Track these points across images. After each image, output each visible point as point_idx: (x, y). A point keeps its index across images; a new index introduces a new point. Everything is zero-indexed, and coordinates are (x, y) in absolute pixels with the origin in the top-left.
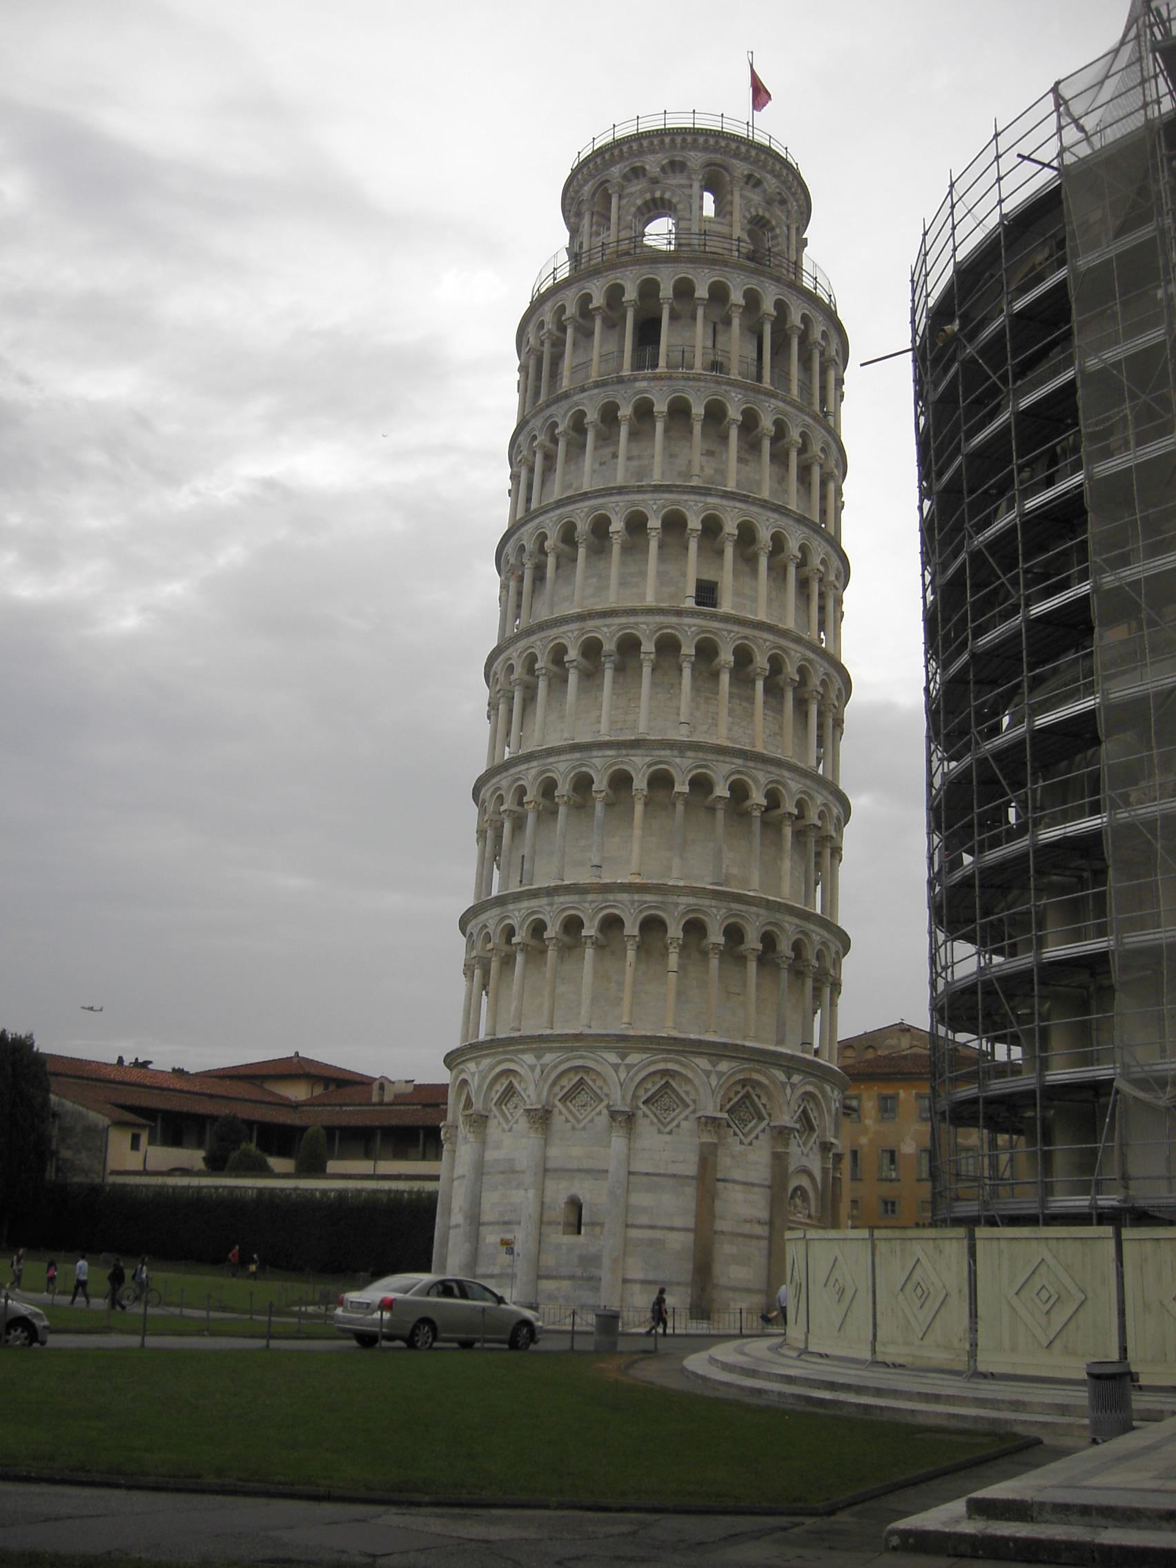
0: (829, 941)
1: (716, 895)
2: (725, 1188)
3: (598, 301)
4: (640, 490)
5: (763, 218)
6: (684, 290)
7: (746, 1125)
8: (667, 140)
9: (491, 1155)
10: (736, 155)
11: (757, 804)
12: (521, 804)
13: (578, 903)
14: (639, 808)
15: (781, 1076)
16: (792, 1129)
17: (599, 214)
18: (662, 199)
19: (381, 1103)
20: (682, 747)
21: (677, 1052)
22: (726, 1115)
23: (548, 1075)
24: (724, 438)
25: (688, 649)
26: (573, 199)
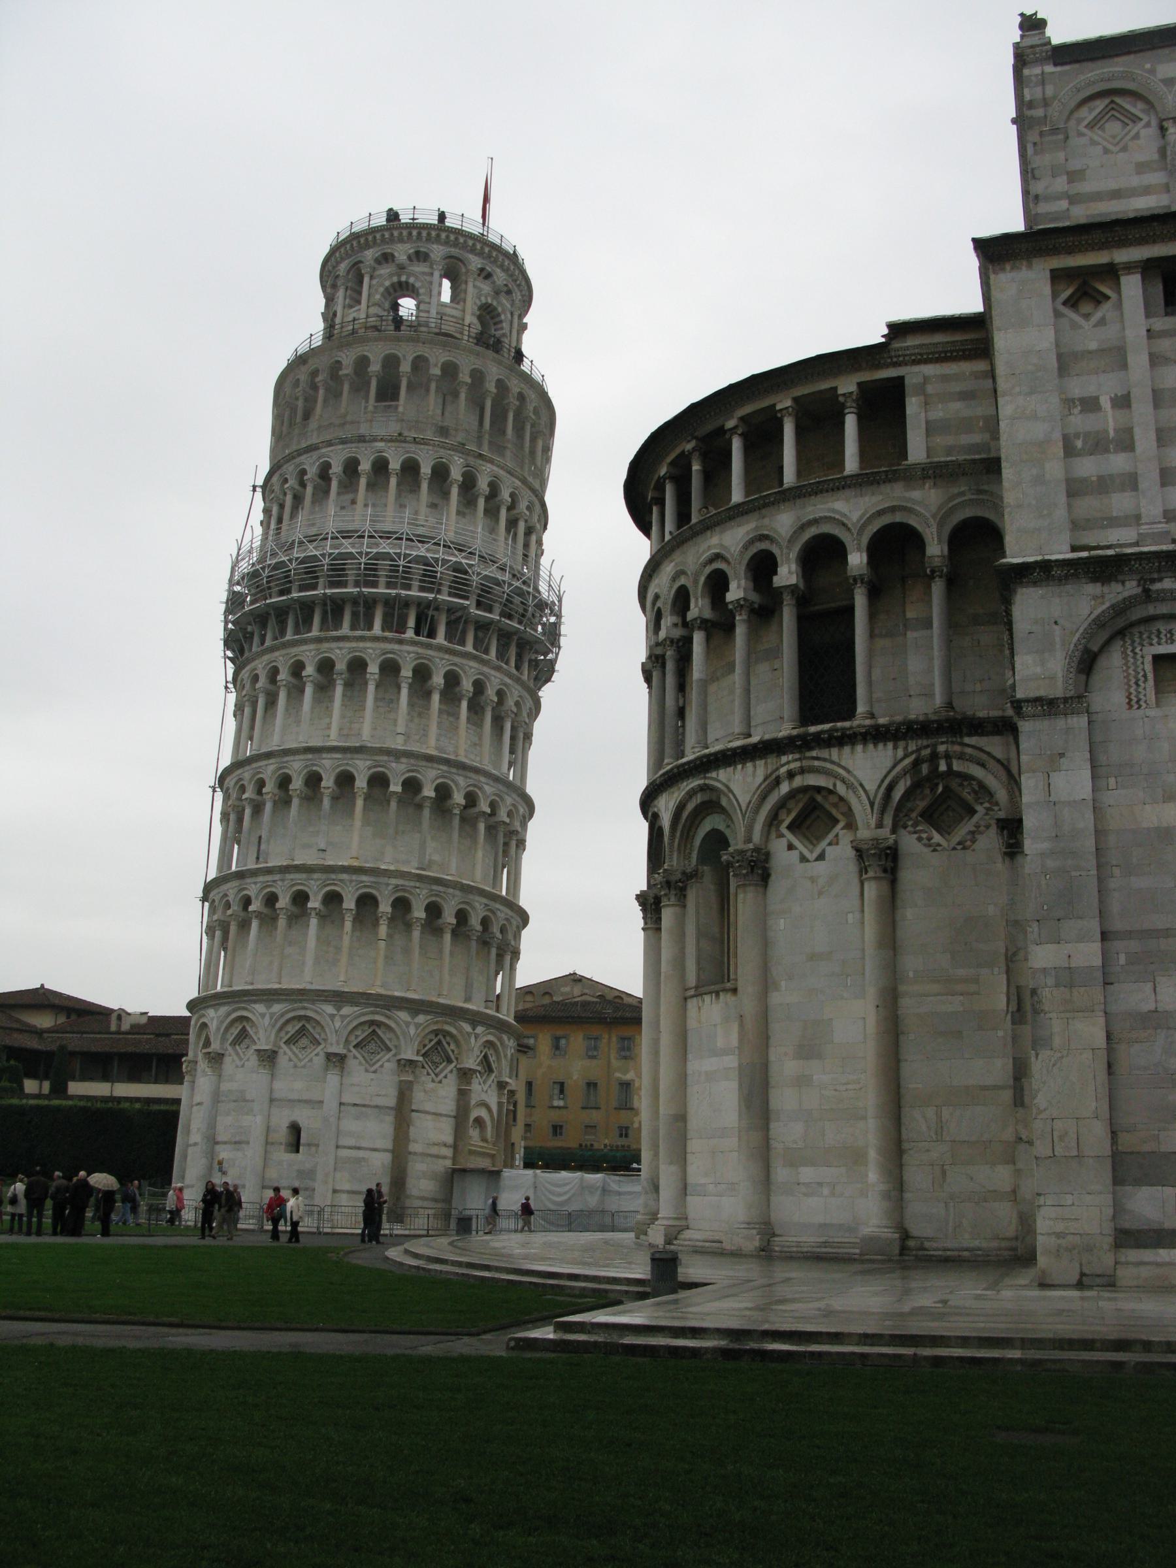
1: (420, 878)
3: (347, 370)
6: (419, 363)
8: (415, 233)
9: (225, 1086)
10: (473, 250)
12: (260, 793)
14: (360, 803)
15: (467, 1027)
16: (475, 1071)
17: (352, 289)
18: (407, 283)
19: (118, 1032)
20: (397, 754)
22: (421, 1059)
23: (276, 1021)
24: (446, 495)
25: (407, 673)
26: (330, 272)
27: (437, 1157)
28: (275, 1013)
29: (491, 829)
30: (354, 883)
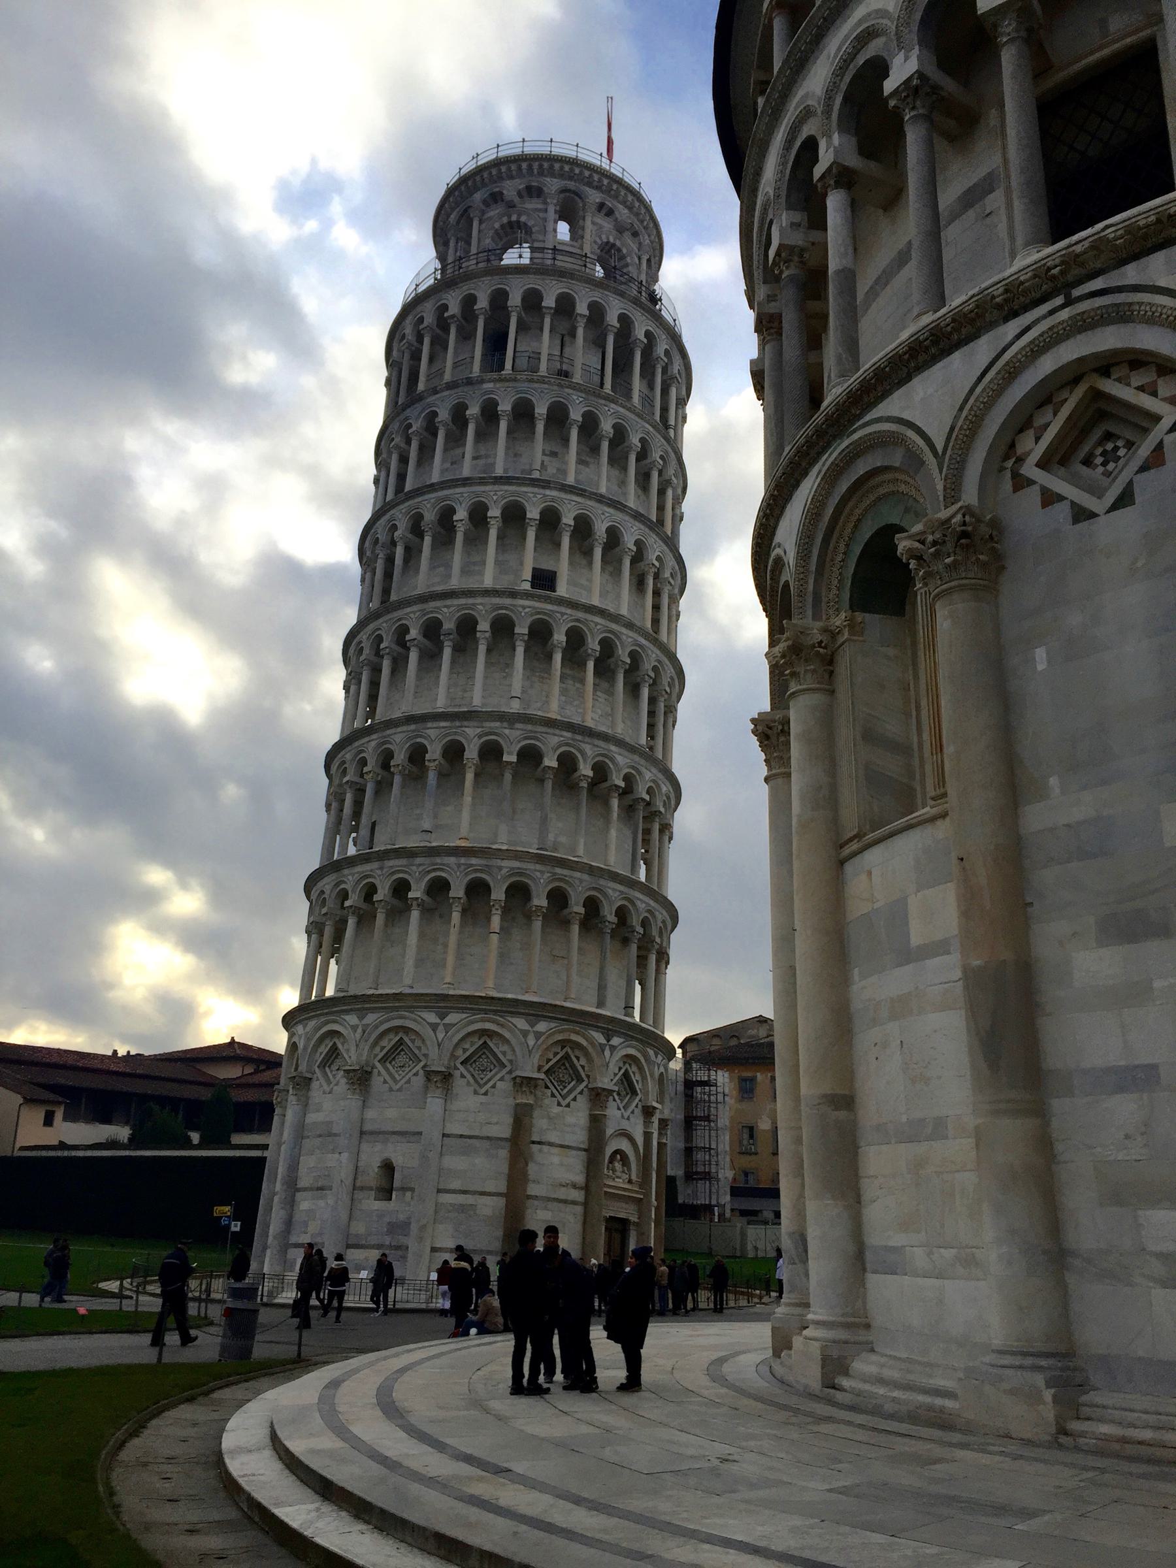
0: (655, 909)
1: (540, 859)
2: (540, 1151)
4: (482, 481)
5: (613, 245)
6: (532, 300)
7: (565, 1087)
8: (524, 165)
9: (311, 1118)
10: (590, 184)
11: (584, 776)
12: (362, 776)
13: (405, 866)
16: (610, 1092)
18: (518, 222)
21: (495, 1012)
22: (542, 1076)
23: (370, 1034)
24: (566, 441)
25: (522, 629)
27: (565, 1202)
28: (368, 1025)
29: (629, 810)
30: (463, 867)
